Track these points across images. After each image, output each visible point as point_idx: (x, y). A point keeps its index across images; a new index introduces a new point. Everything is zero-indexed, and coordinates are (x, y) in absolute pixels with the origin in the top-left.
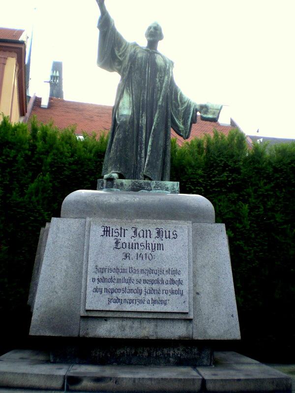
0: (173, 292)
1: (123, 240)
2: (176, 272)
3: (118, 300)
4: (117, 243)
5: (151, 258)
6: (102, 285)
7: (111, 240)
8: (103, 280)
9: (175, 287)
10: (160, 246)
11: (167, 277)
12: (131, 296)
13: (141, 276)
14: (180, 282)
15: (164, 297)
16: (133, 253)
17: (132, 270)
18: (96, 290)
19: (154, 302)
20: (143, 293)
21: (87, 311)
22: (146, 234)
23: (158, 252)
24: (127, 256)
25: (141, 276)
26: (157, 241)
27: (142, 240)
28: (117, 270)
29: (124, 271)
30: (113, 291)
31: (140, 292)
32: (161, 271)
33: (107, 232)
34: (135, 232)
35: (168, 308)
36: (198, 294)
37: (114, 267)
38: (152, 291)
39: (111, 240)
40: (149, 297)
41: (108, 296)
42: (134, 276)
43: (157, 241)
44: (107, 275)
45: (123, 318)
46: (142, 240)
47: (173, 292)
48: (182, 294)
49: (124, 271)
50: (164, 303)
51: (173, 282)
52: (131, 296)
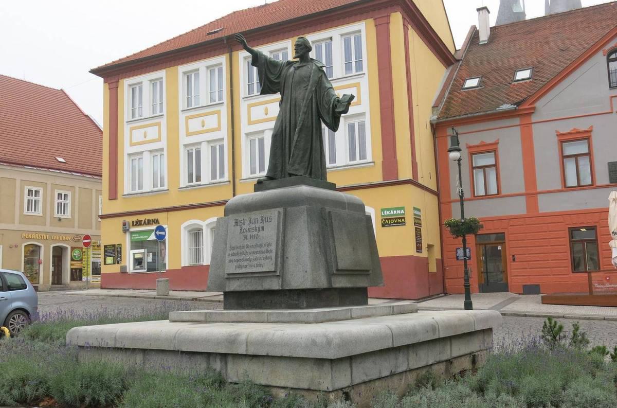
0: (267, 258)
1: (244, 227)
2: (269, 245)
3: (240, 267)
4: (241, 230)
5: (257, 237)
6: (233, 258)
7: (238, 228)
8: (233, 255)
9: (268, 255)
10: (262, 229)
11: (264, 249)
12: (245, 263)
13: (252, 250)
14: (271, 251)
15: (262, 262)
16: (248, 234)
17: (248, 246)
18: (230, 261)
19: (257, 266)
20: (252, 260)
21: (228, 274)
22: (256, 221)
23: (261, 233)
24: (245, 237)
25: (252, 250)
26: (261, 225)
27: (253, 226)
28: (241, 247)
29: (243, 247)
30: (238, 261)
31: (250, 260)
32: (261, 245)
33: (237, 223)
34: (250, 221)
35: (264, 270)
36: (287, 258)
37: (238, 245)
38: (256, 259)
39: (238, 228)
40: (255, 263)
41: (235, 264)
42: (248, 250)
43: (261, 225)
44: (235, 251)
45: (247, 277)
46: (253, 226)
47: (267, 258)
48: (271, 259)
49: (243, 247)
50: (262, 266)
51: (267, 251)
52: (245, 263)
